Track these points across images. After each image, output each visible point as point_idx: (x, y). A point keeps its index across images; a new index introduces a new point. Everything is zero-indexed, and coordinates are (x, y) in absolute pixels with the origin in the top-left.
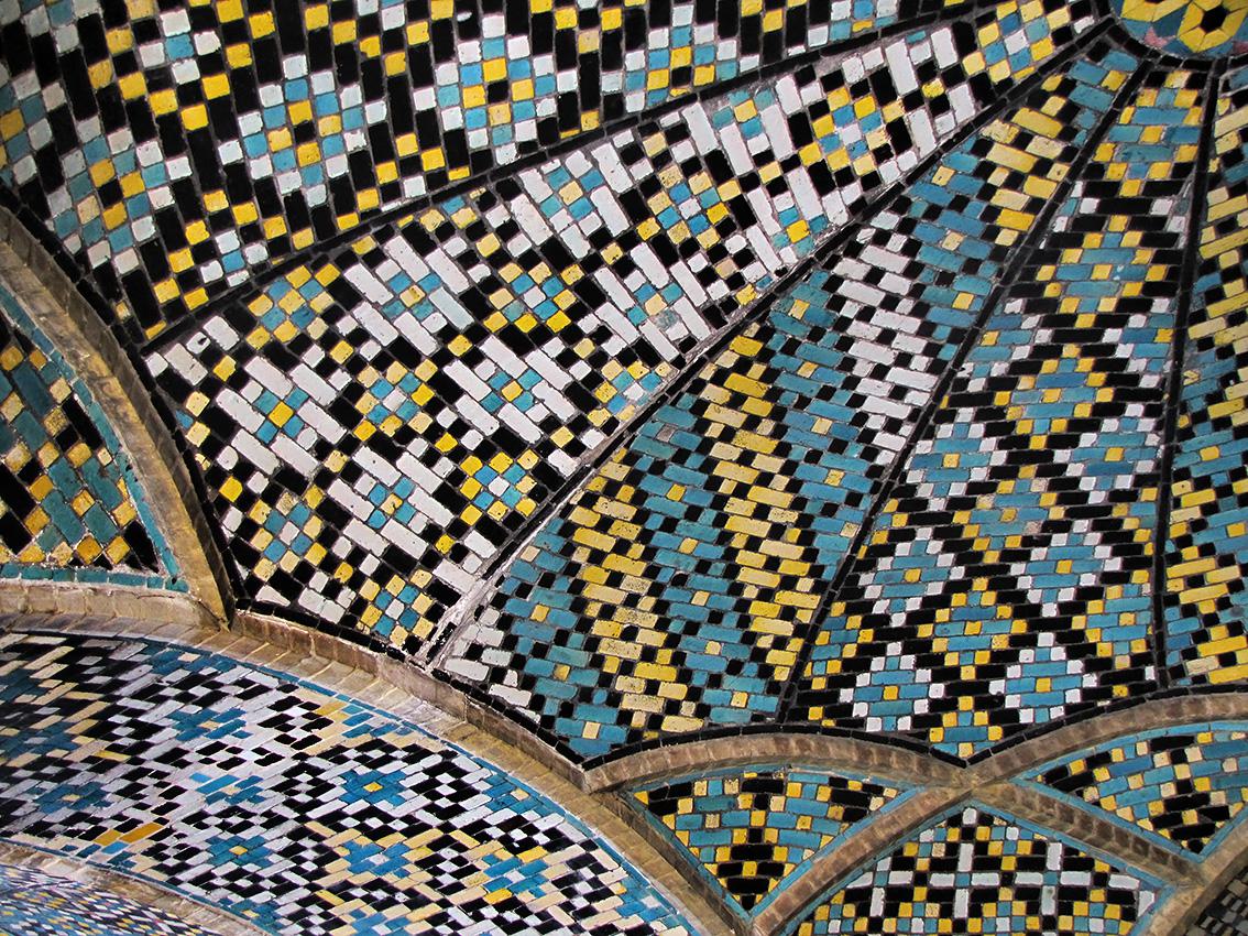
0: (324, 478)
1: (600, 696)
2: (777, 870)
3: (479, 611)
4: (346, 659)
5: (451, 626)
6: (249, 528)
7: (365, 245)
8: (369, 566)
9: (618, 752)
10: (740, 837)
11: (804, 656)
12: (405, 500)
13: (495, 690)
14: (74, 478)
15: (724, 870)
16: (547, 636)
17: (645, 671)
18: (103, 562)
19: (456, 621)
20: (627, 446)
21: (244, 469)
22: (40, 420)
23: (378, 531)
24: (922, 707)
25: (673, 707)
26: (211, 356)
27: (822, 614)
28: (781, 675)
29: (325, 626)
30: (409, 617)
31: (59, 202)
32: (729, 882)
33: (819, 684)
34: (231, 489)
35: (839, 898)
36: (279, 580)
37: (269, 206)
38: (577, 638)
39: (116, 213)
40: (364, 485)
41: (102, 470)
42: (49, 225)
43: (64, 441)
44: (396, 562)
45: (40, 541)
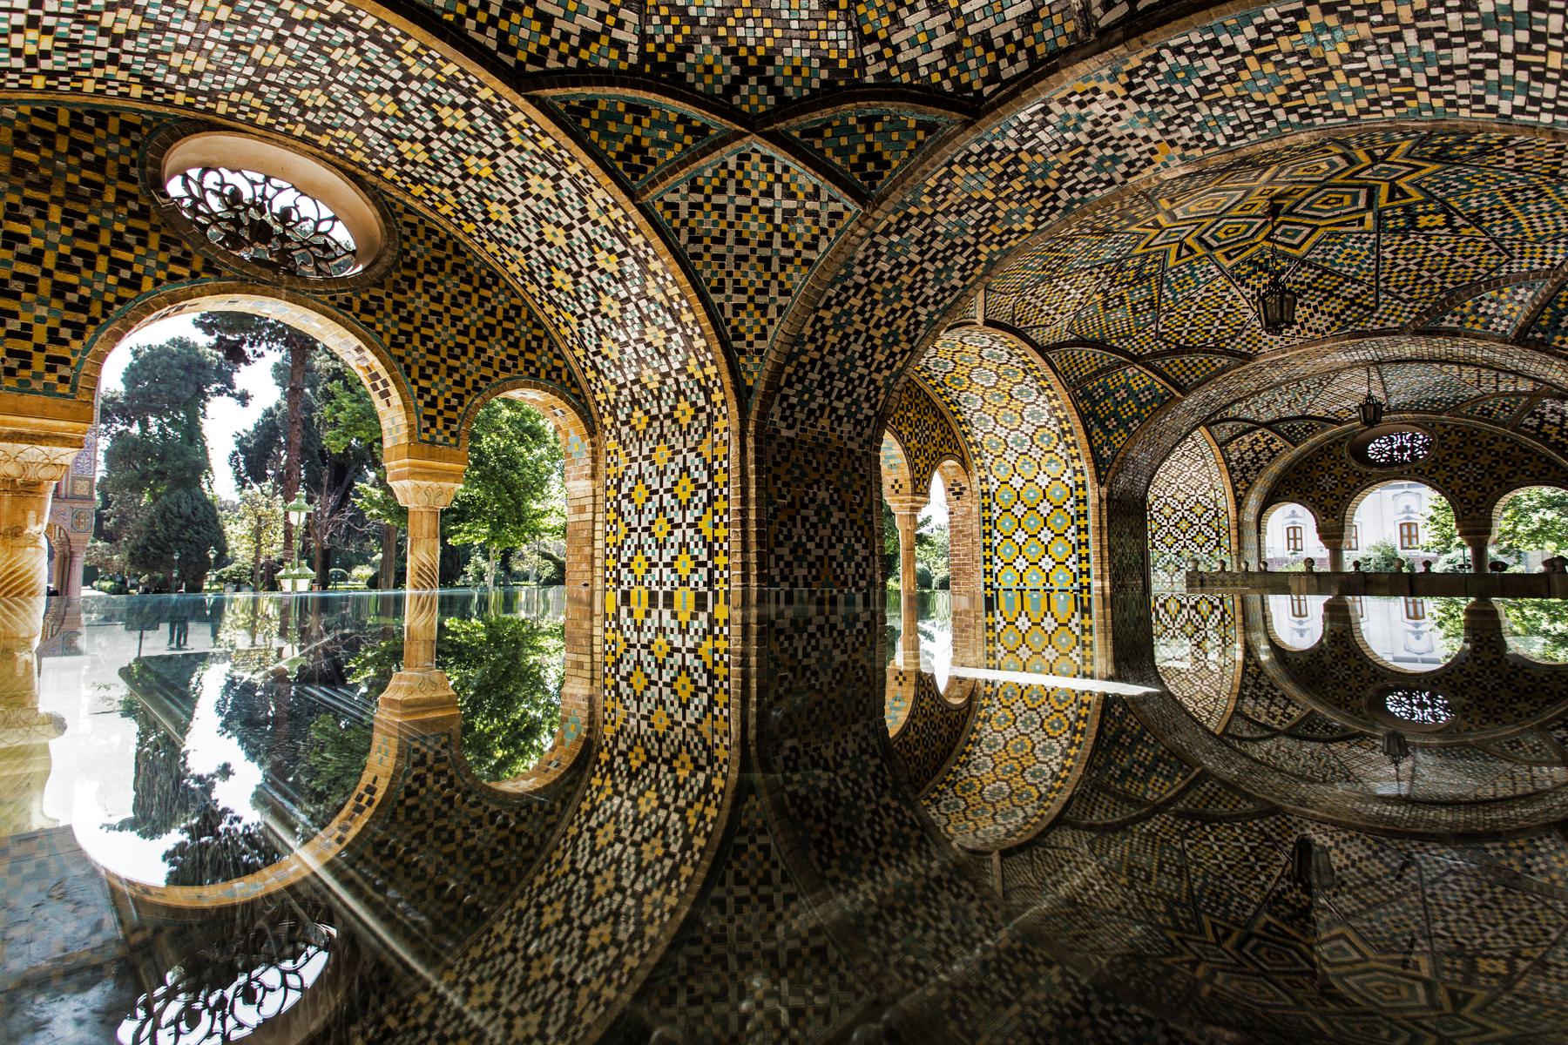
8: (1017, 35)
14: (885, 133)
18: (920, 143)
26: (879, 56)
31: (789, 91)
36: (987, 81)
39: (805, 72)
43: (870, 130)
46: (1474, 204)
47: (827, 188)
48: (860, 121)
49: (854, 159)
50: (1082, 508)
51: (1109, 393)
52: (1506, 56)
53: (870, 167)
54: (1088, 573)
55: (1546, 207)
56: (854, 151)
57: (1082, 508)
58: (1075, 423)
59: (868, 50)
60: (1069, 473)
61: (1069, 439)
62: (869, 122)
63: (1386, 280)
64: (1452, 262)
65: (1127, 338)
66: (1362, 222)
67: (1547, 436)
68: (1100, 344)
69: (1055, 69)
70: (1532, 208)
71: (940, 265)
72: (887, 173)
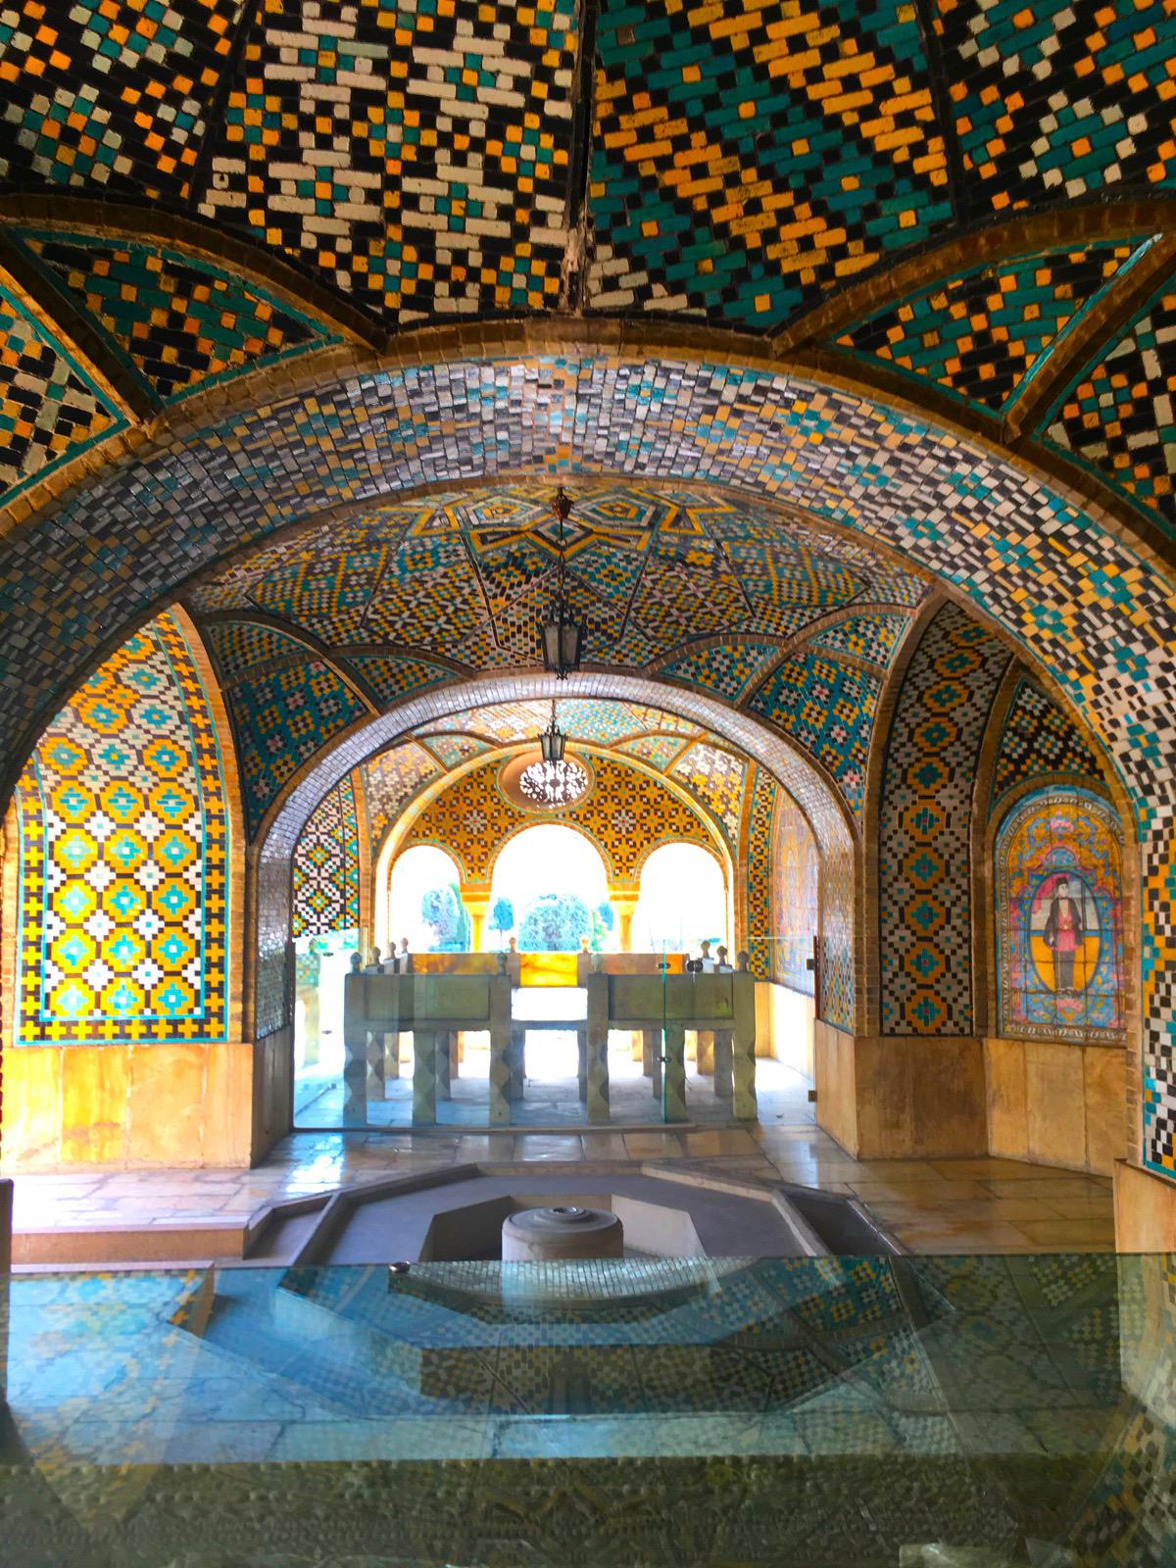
0: (393, 216)
1: (757, 271)
2: (1019, 364)
3: (590, 253)
4: (494, 336)
5: (572, 274)
6: (359, 279)
7: (253, 52)
9: (797, 312)
10: (966, 345)
11: (953, 152)
12: (466, 199)
13: (649, 305)
14: (209, 311)
15: (958, 379)
16: (671, 244)
17: (789, 232)
18: (270, 349)
19: (576, 268)
20: (599, 66)
21: (326, 241)
22: (157, 288)
23: (463, 231)
24: (1126, 149)
25: (838, 252)
26: (237, 183)
27: (942, 103)
28: (939, 179)
29: (467, 317)
30: (534, 283)
31: (43, 165)
32: (969, 389)
33: (988, 171)
34: (327, 260)
35: (1100, 373)
36: (408, 302)
37: (164, 75)
38: (701, 233)
39: (86, 145)
40: (426, 204)
41: (225, 294)
42: (52, 182)
43: (184, 291)
44: (492, 248)
45: (218, 356)
46: (743, 553)
47: (76, 357)
48: (168, 269)
49: (141, 331)
50: (215, 879)
51: (279, 697)
52: (943, 508)
53: (169, 354)
54: (220, 990)
55: (798, 575)
56: (145, 318)
57: (215, 879)
58: (224, 736)
59: (220, 164)
60: (199, 818)
61: (208, 763)
62: (187, 279)
63: (637, 610)
64: (703, 605)
65: (321, 618)
66: (639, 537)
67: (696, 786)
68: (283, 620)
69: (518, 335)
70: (787, 573)
71: (201, 521)
72: (197, 375)
